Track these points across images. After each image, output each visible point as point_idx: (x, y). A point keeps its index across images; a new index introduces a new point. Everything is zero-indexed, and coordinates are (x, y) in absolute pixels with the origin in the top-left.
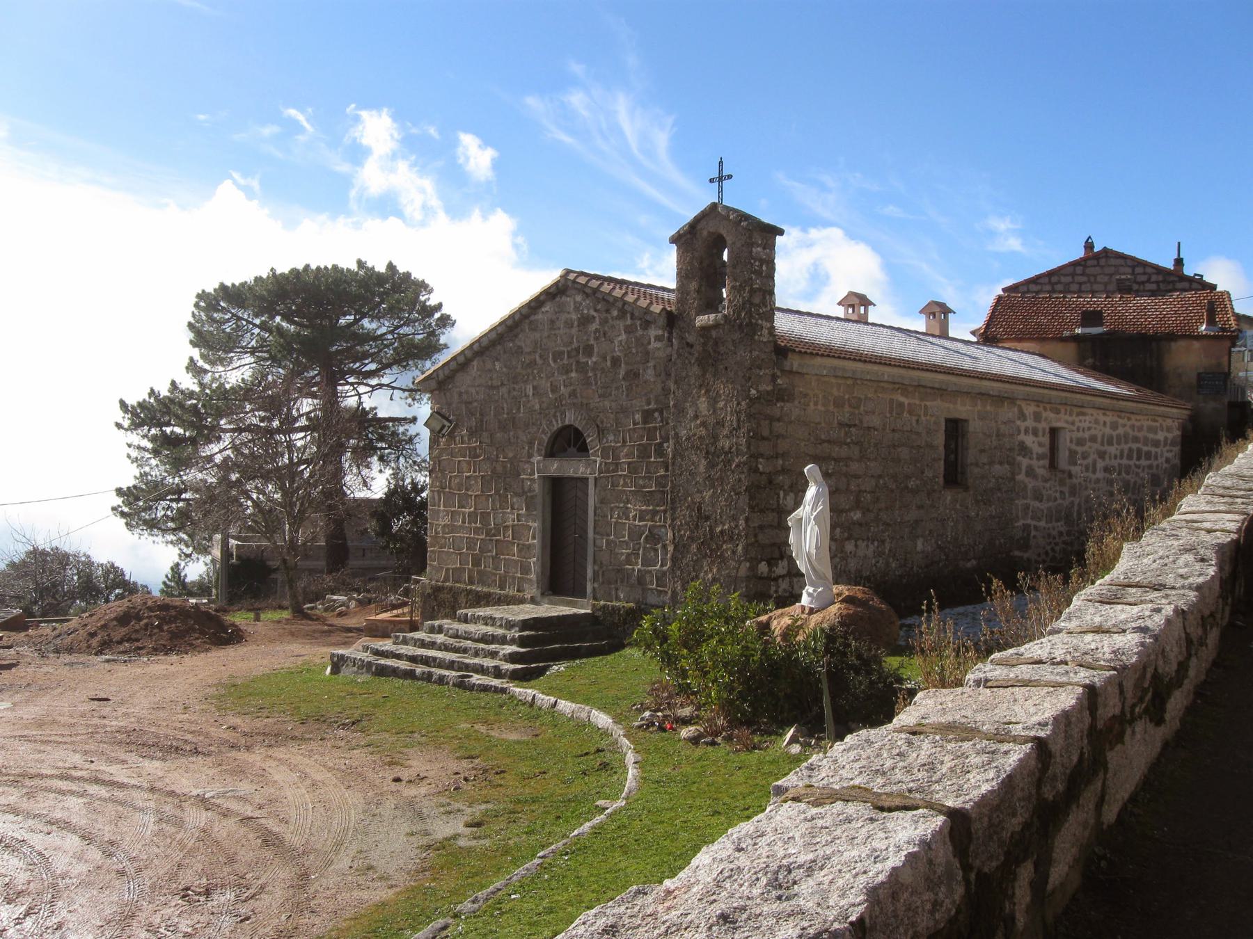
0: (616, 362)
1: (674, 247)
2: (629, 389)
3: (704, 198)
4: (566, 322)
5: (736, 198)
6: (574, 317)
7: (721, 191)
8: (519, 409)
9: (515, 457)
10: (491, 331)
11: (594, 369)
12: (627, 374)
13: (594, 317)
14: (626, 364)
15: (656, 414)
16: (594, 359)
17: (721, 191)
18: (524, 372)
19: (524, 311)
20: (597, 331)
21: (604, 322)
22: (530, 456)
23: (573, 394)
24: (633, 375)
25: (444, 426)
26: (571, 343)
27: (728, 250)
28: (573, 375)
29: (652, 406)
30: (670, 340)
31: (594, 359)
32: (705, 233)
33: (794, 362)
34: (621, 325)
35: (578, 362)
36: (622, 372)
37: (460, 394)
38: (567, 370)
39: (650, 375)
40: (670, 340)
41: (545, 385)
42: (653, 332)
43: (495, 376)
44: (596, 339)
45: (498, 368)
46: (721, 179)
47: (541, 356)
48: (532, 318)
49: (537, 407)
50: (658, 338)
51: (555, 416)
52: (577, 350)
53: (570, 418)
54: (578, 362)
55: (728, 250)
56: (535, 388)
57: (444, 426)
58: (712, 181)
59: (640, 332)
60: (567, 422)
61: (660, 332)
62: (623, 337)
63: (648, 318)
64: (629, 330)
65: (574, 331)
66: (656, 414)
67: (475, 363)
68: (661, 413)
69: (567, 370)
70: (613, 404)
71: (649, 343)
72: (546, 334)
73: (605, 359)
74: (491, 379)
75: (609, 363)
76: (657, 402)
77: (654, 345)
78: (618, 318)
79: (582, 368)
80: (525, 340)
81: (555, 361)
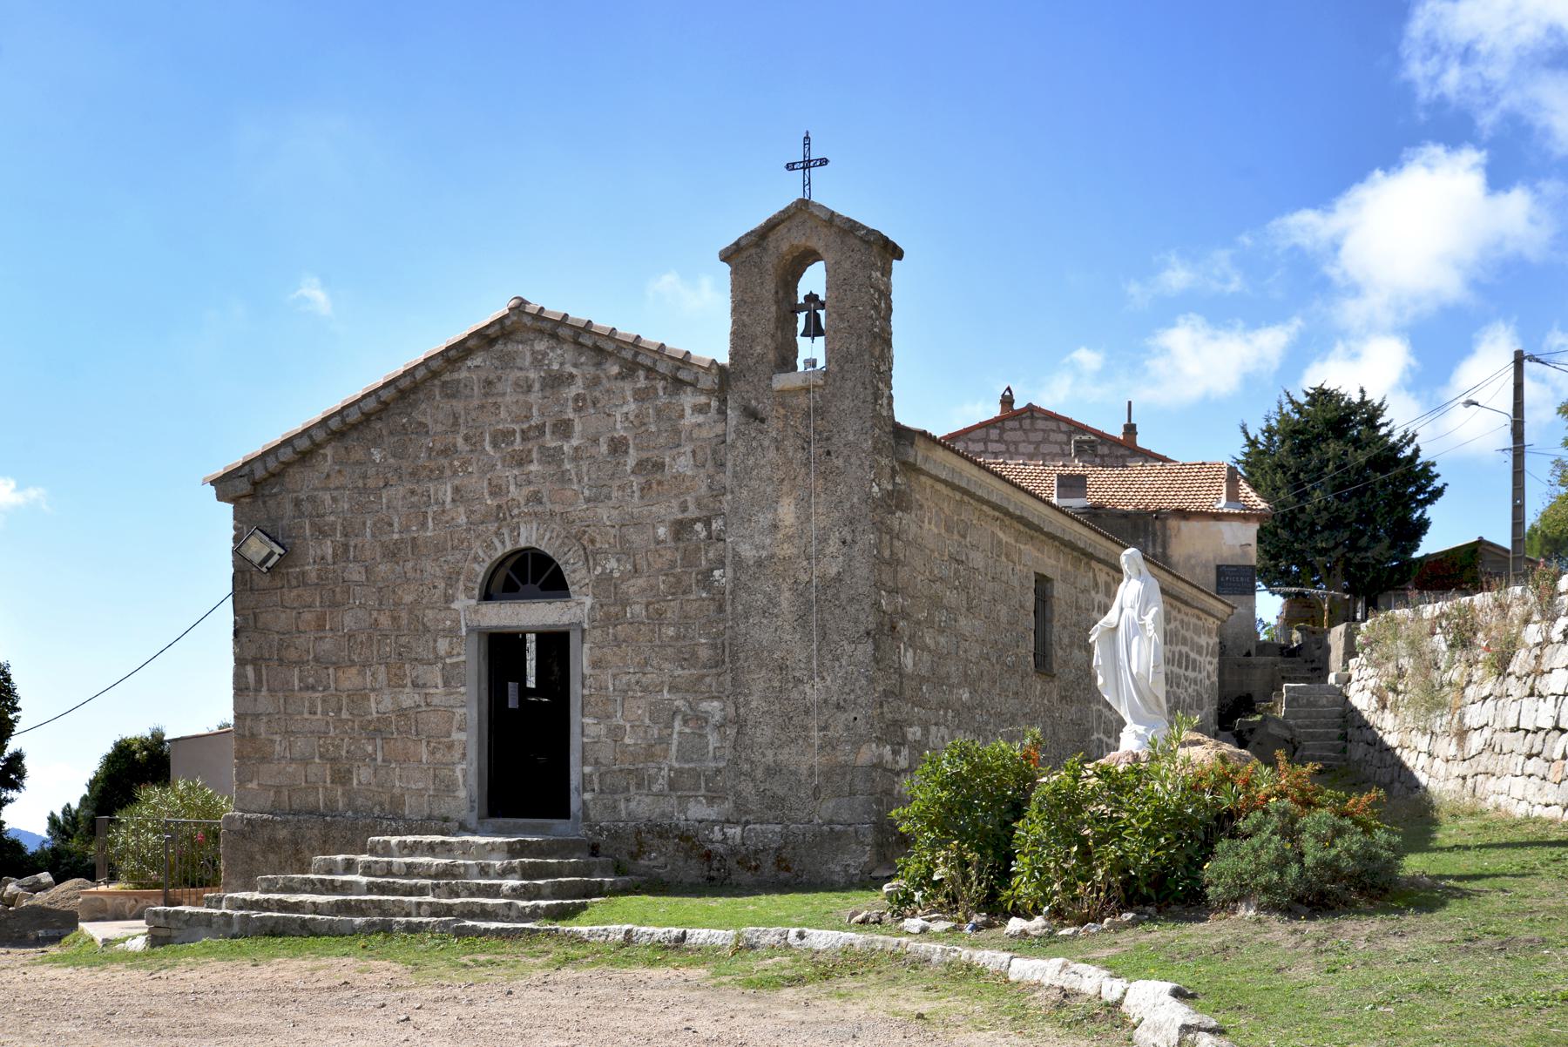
0: (618, 447)
1: (726, 268)
2: (645, 489)
3: (787, 192)
4: (516, 384)
5: (836, 194)
6: (532, 375)
7: (807, 184)
8: (423, 525)
9: (416, 602)
10: (386, 385)
11: (575, 459)
12: (640, 464)
13: (572, 376)
14: (639, 448)
15: (699, 527)
16: (575, 442)
17: (807, 184)
18: (432, 465)
19: (434, 365)
20: (577, 398)
21: (595, 382)
22: (449, 599)
23: (536, 498)
24: (651, 467)
25: (271, 554)
26: (528, 418)
27: (814, 275)
28: (534, 467)
29: (693, 512)
30: (722, 412)
31: (575, 442)
32: (785, 247)
33: (918, 454)
34: (627, 387)
35: (542, 448)
36: (631, 461)
37: (297, 503)
38: (521, 460)
39: (683, 464)
40: (722, 412)
41: (477, 484)
42: (688, 400)
43: (372, 471)
44: (578, 410)
45: (377, 457)
46: (807, 164)
47: (467, 439)
48: (446, 377)
49: (462, 520)
50: (700, 409)
51: (498, 534)
52: (541, 429)
53: (529, 536)
54: (542, 448)
55: (814, 275)
56: (456, 490)
57: (271, 554)
58: (790, 167)
59: (663, 399)
60: (523, 544)
61: (703, 399)
62: (632, 407)
63: (682, 375)
64: (641, 396)
65: (535, 397)
66: (699, 527)
67: (329, 451)
68: (707, 523)
69: (521, 460)
70: (615, 513)
71: (682, 416)
72: (476, 402)
73: (595, 441)
74: (365, 477)
75: (604, 448)
76: (699, 505)
77: (690, 419)
78: (621, 377)
79: (552, 457)
80: (432, 412)
81: (495, 445)
